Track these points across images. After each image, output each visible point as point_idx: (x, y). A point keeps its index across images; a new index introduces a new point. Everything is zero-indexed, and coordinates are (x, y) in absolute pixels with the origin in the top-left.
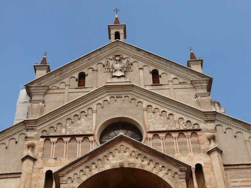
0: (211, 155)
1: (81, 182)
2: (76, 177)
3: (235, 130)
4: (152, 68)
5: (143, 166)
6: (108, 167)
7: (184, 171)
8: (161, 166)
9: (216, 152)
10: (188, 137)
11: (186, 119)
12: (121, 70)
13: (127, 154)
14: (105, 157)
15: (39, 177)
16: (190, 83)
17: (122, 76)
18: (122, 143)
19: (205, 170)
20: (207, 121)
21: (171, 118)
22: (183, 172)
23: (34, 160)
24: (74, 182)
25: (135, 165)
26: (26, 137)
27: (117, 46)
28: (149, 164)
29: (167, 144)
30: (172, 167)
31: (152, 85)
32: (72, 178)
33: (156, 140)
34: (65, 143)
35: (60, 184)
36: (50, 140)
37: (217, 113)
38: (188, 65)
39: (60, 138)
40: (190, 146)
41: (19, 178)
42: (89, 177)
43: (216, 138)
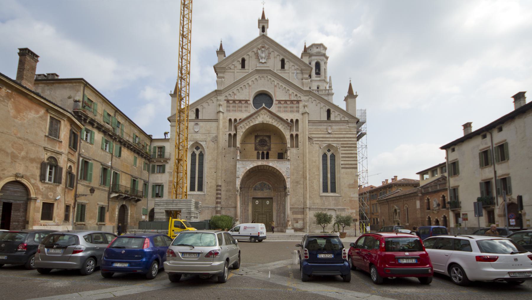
3: (318, 101)
4: (281, 57)
11: (295, 93)
12: (264, 58)
16: (300, 69)
17: (265, 63)
19: (300, 122)
20: (305, 96)
21: (288, 92)
23: (223, 113)
26: (218, 100)
27: (263, 38)
29: (285, 107)
31: (281, 70)
33: (279, 105)
36: (229, 102)
38: (302, 57)
39: (234, 101)
40: (295, 109)
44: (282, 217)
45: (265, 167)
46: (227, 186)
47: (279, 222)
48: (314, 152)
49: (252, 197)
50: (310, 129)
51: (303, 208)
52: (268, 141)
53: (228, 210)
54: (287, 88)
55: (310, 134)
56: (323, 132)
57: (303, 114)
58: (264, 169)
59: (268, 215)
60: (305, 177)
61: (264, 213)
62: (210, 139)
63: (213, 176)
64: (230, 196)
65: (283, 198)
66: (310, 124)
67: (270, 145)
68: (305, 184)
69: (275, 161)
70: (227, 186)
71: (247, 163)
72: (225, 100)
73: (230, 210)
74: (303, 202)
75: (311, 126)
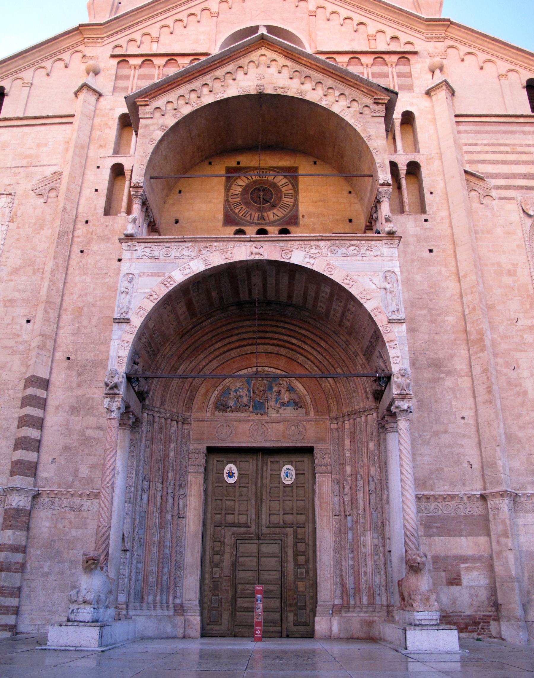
0: (434, 98)
1: (180, 117)
2: (170, 107)
5: (301, 93)
6: (232, 91)
7: (382, 104)
8: (337, 93)
9: (444, 91)
10: (392, 65)
11: (390, 32)
13: (273, 70)
14: (228, 75)
15: (107, 124)
18: (263, 51)
22: (380, 106)
24: (166, 116)
25: (286, 91)
28: (314, 89)
30: (360, 96)
32: (163, 109)
34: (157, 68)
35: (139, 119)
37: (452, 23)
41: (70, 125)
42: (196, 108)
43: (445, 69)
44: (369, 550)
45: (271, 280)
46: (79, 385)
47: (350, 581)
48: (499, 231)
49: (205, 446)
50: (465, 145)
51: (483, 497)
52: (287, 189)
53: (72, 509)
54: (358, 18)
55: (470, 162)
56: (524, 157)
57: (428, 93)
58: (269, 303)
59: (290, 541)
60: (474, 336)
61: (265, 530)
62: (30, 187)
63: (18, 335)
64: (90, 433)
65: (372, 445)
66: (462, 128)
67: (296, 205)
68: (477, 370)
69: (322, 244)
70: (79, 385)
71: (174, 253)
72: (113, 56)
73: (79, 510)
74: (476, 465)
75: (473, 135)
